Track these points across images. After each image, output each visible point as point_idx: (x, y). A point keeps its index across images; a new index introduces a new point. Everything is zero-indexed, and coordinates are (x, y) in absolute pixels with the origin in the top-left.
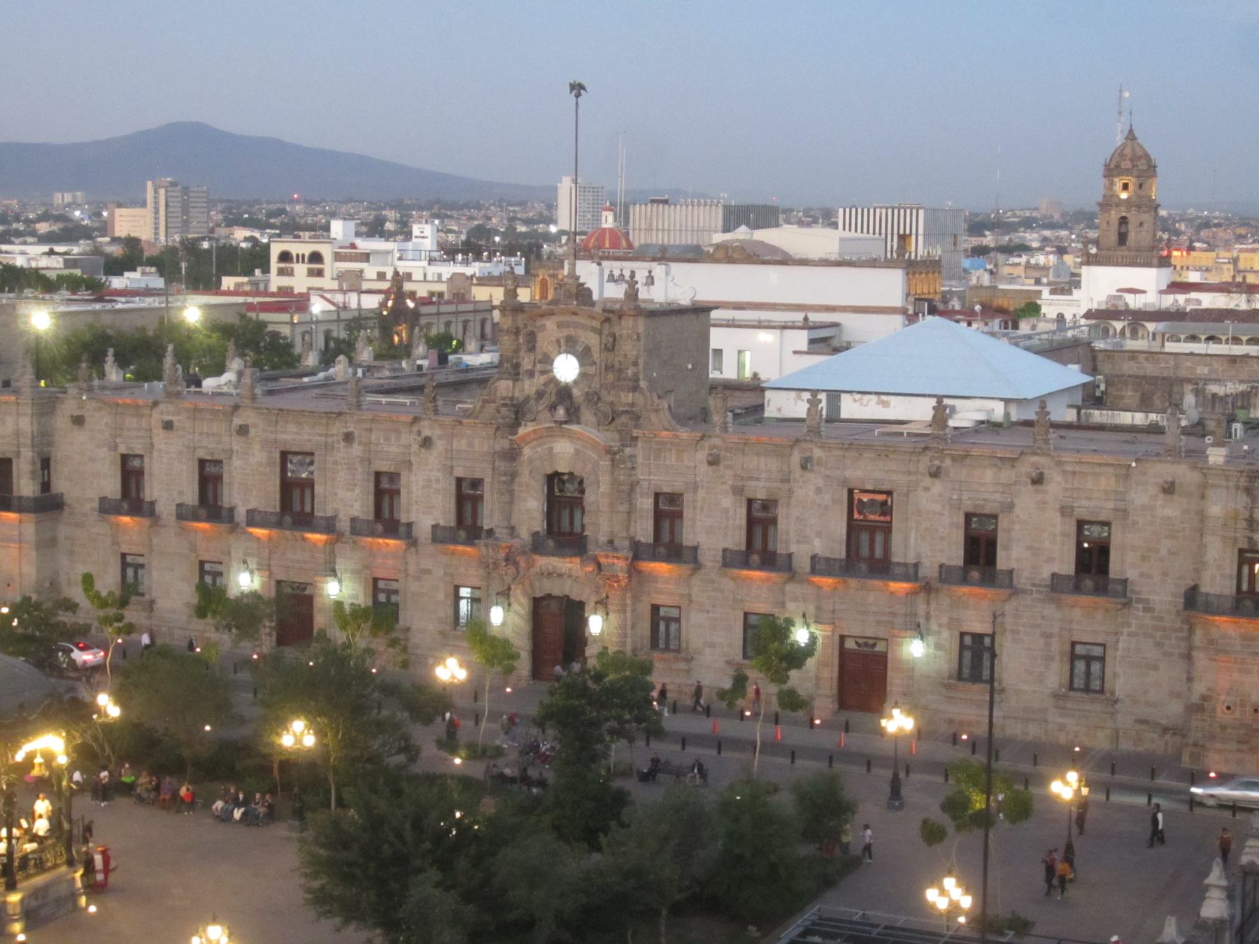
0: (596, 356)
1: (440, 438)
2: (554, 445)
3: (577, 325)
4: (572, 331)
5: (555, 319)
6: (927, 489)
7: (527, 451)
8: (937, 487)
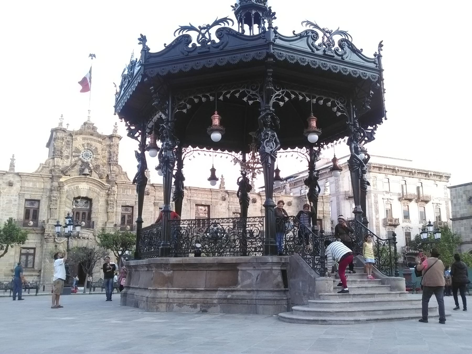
0: (100, 152)
1: (18, 182)
2: (80, 185)
3: (91, 139)
4: (89, 142)
5: (82, 136)
6: (221, 204)
7: (66, 187)
8: (224, 204)
